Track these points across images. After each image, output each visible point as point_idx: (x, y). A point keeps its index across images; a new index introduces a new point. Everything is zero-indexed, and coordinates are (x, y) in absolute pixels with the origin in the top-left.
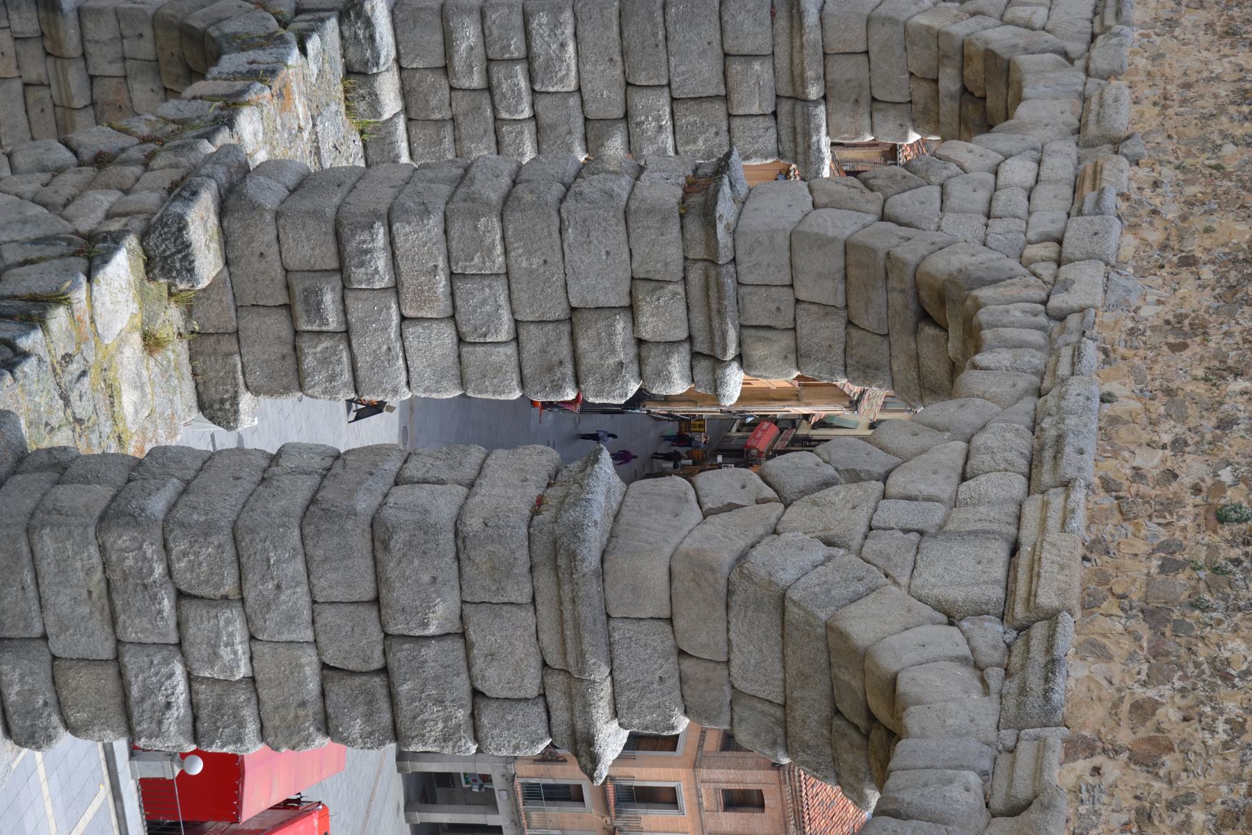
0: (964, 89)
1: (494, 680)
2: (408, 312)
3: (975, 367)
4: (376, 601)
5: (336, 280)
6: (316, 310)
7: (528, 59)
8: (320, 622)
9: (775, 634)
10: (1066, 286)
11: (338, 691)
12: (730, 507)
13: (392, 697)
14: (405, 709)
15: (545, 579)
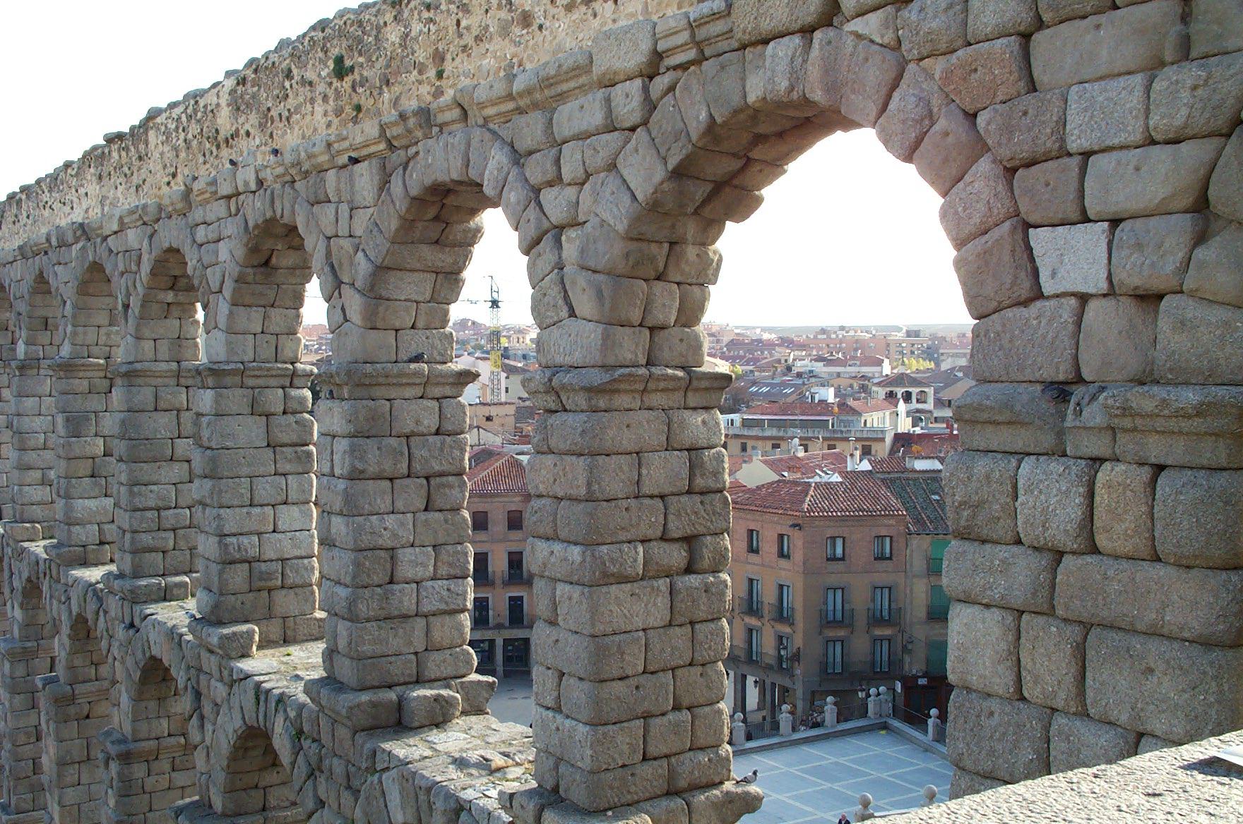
0: (172, 288)
1: (430, 422)
2: (271, 528)
3: (282, 216)
4: (391, 480)
5: (255, 565)
6: (269, 576)
7: (158, 510)
8: (402, 509)
9: (399, 274)
10: (246, 183)
11: (439, 502)
12: (343, 309)
13: (442, 475)
14: (446, 467)
15: (377, 392)
